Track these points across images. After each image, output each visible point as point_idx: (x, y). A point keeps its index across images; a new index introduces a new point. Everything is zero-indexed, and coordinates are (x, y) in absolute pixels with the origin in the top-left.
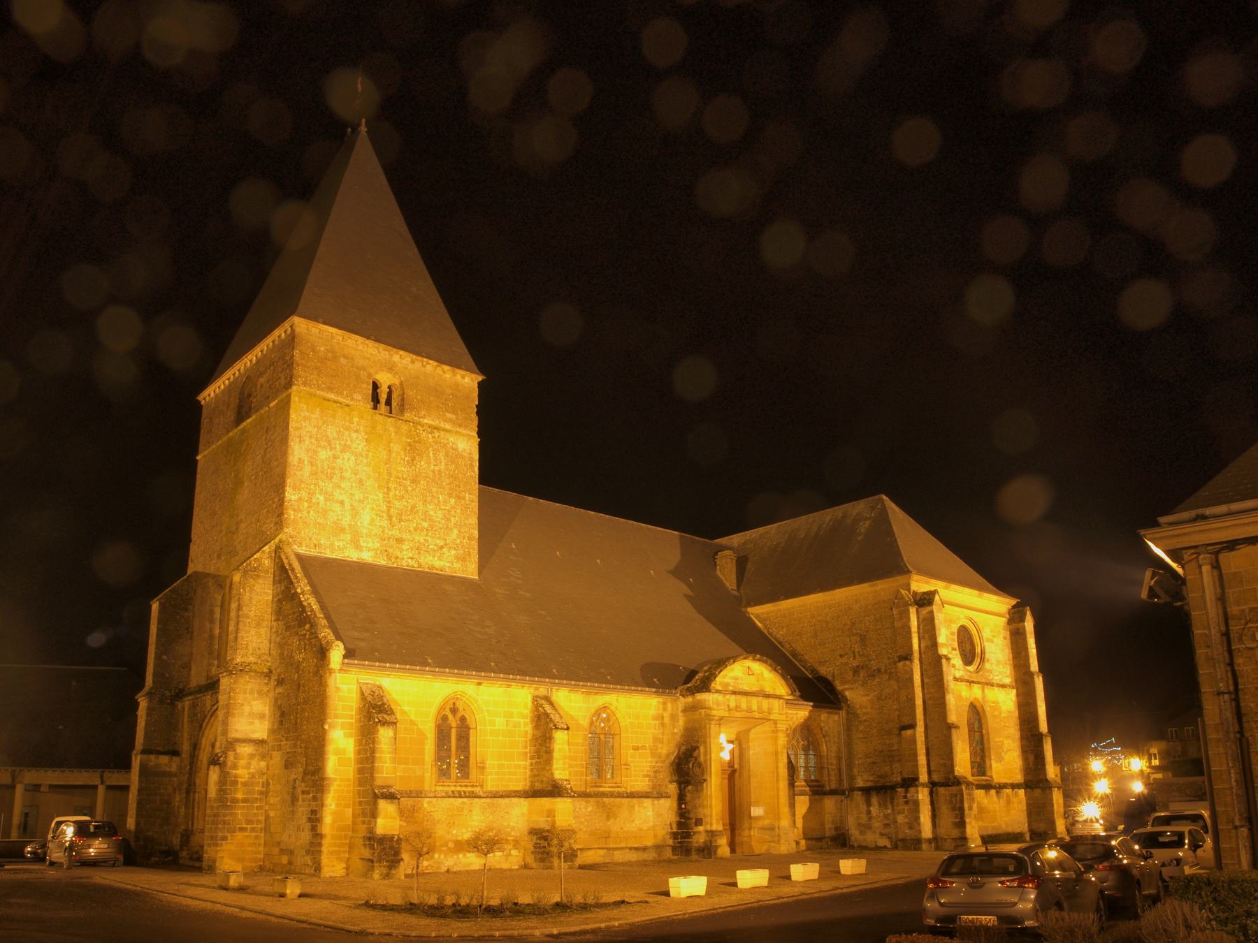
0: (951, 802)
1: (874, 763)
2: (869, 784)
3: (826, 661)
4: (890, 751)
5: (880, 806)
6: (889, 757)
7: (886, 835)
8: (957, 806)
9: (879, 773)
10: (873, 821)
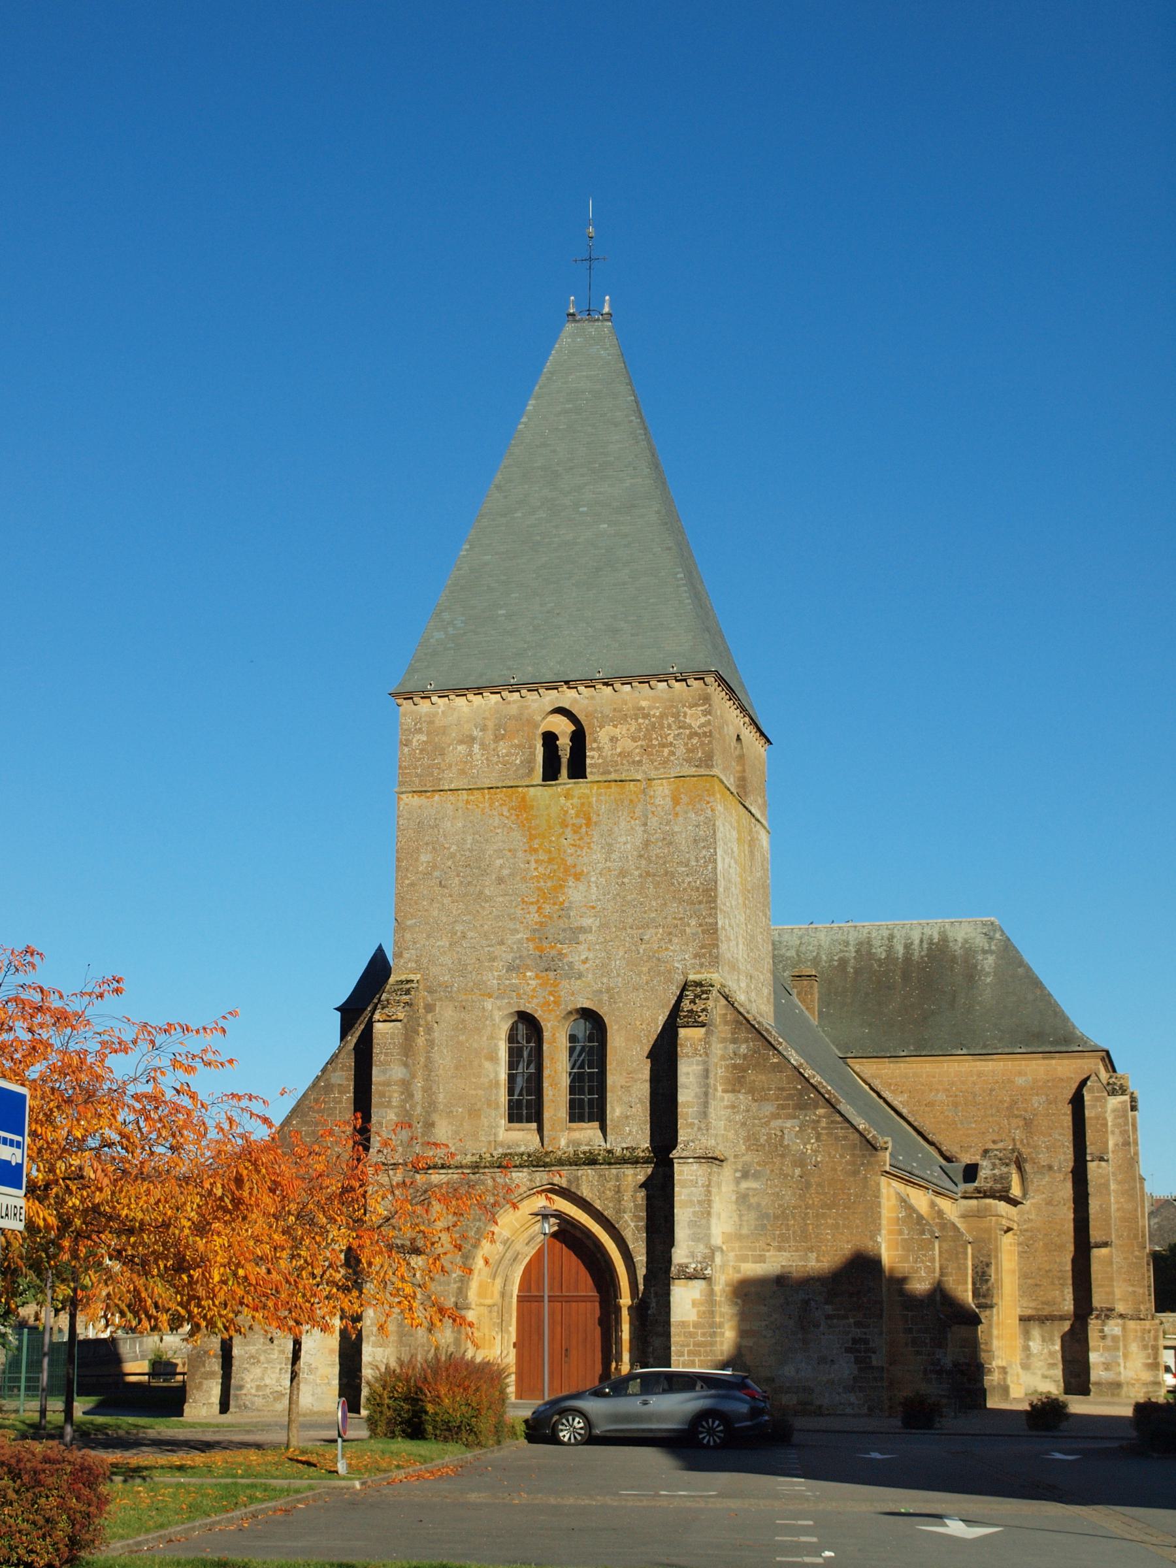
0: (1143, 1339)
1: (1036, 1285)
2: (1030, 1312)
3: (971, 1147)
4: (1061, 1271)
5: (1043, 1341)
6: (1060, 1278)
7: (1051, 1378)
8: (1150, 1344)
9: (1044, 1299)
10: (1033, 1360)
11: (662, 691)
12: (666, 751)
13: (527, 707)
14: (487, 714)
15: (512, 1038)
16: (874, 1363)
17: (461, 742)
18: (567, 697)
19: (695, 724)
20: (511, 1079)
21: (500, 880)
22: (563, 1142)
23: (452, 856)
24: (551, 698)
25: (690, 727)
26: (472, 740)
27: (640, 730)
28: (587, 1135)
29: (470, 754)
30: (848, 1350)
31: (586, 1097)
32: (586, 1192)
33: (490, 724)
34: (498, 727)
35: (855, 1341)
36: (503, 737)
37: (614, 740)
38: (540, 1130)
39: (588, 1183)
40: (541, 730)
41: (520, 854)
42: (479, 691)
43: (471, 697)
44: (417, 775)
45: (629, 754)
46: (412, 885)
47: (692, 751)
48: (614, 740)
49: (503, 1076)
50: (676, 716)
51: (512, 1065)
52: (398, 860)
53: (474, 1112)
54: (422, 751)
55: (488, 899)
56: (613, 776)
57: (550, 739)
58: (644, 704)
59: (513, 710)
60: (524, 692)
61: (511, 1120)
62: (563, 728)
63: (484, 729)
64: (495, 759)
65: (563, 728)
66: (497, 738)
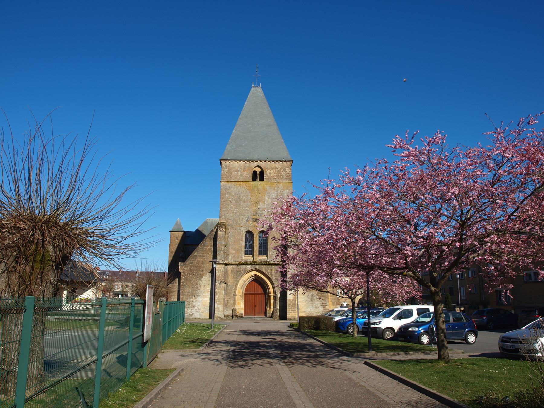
11: (281, 164)
12: (282, 177)
13: (251, 165)
14: (242, 166)
15: (246, 236)
16: (327, 308)
17: (236, 171)
18: (260, 163)
19: (288, 171)
20: (246, 245)
21: (244, 202)
22: (258, 260)
23: (233, 196)
24: (256, 164)
25: (287, 172)
26: (239, 171)
27: (276, 171)
28: (263, 258)
29: (238, 174)
30: (321, 305)
31: (262, 250)
32: (264, 271)
33: (242, 168)
34: (244, 169)
35: (323, 303)
36: (245, 171)
37: (270, 173)
38: (253, 257)
39: (264, 268)
40: (253, 170)
41: (249, 196)
42: (240, 161)
43: (238, 162)
44: (225, 178)
45: (274, 177)
46: (224, 201)
47: (287, 177)
48: (270, 173)
49: (244, 245)
50: (284, 169)
51: (245, 243)
52: (221, 196)
53: (238, 253)
54: (227, 172)
55: (242, 206)
56: (270, 181)
57: (255, 173)
58: (277, 166)
59: (248, 165)
60: (250, 161)
61: (245, 254)
62: (258, 170)
63: (241, 169)
64: (243, 175)
65: (258, 170)
66: (244, 171)
